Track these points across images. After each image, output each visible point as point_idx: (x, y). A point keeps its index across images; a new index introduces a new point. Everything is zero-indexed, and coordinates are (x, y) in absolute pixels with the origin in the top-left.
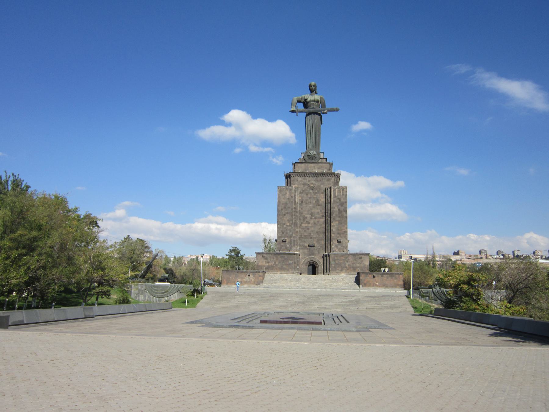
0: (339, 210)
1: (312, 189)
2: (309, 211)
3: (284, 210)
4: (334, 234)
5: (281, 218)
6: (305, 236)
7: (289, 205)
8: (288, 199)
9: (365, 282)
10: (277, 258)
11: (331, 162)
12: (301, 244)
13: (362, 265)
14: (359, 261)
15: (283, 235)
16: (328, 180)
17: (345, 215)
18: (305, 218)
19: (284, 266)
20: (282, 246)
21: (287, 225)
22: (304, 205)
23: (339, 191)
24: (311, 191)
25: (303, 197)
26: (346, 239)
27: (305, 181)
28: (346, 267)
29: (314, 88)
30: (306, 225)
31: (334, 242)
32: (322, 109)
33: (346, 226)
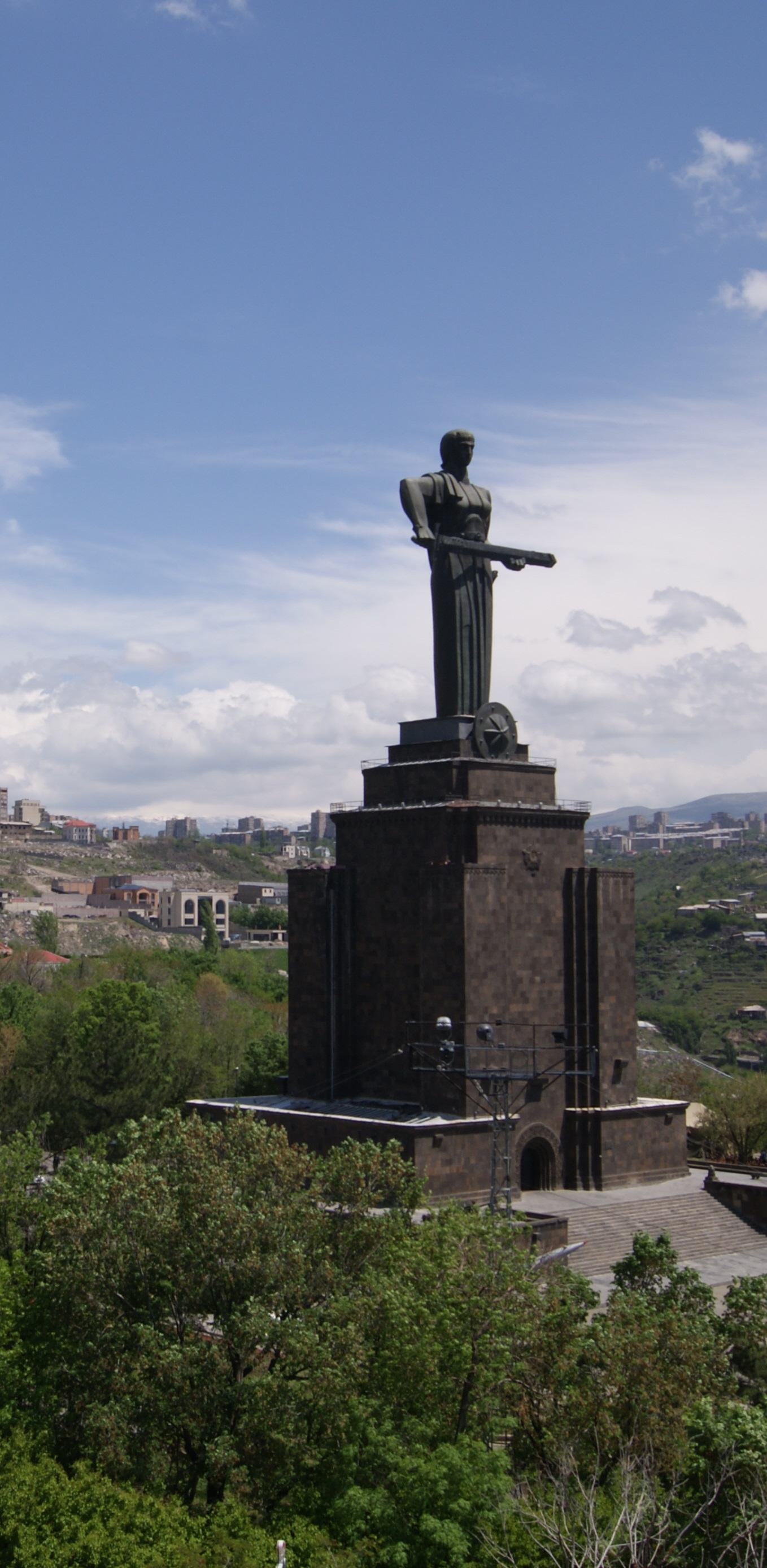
0: (617, 953)
4: (606, 1040)
8: (494, 913)
24: (530, 880)
31: (607, 1070)
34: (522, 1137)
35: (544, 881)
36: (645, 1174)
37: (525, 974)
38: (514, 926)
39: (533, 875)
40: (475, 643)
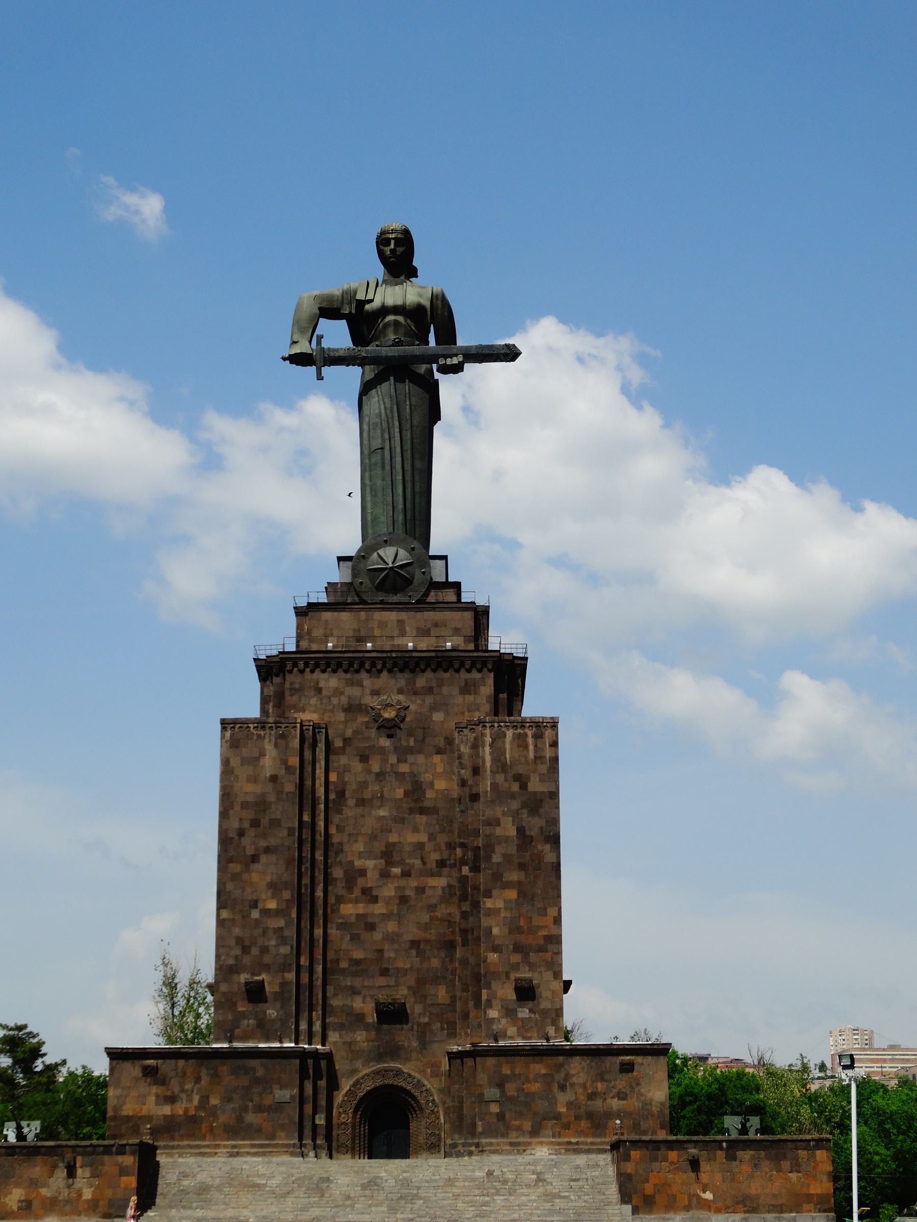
0: (521, 831)
1: (390, 728)
2: (373, 837)
3: (251, 833)
4: (496, 949)
5: (235, 877)
6: (356, 962)
7: (276, 812)
8: (274, 779)
9: (649, 1189)
10: (215, 1076)
11: (480, 602)
12: (335, 1002)
13: (633, 1103)
14: (621, 1082)
15: (247, 960)
16: (468, 689)
17: (550, 858)
18: (354, 875)
19: (251, 1118)
20: (243, 1015)
21: (266, 912)
22: (350, 811)
23: (521, 740)
24: (385, 742)
25: (347, 769)
26: (558, 974)
27: (355, 692)
28: (558, 1117)
29: (400, 250)
30: (361, 908)
32: (443, 349)
33: (552, 912)
35: (412, 743)
36: (569, 1143)
37: (370, 864)
38: (351, 802)
39: (390, 736)
40: (388, 468)
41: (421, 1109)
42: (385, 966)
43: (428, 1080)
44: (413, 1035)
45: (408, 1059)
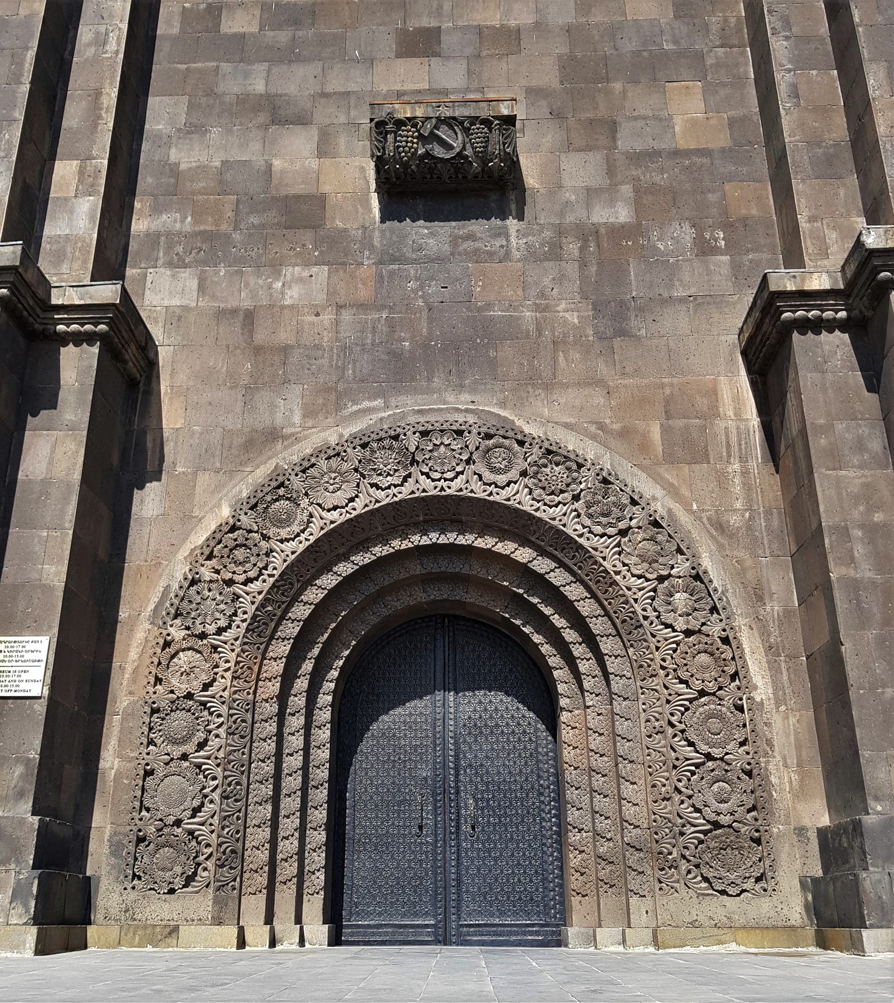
34: (279, 486)
41: (628, 628)
42: (426, 22)
43: (658, 479)
44: (560, 279)
45: (537, 382)
